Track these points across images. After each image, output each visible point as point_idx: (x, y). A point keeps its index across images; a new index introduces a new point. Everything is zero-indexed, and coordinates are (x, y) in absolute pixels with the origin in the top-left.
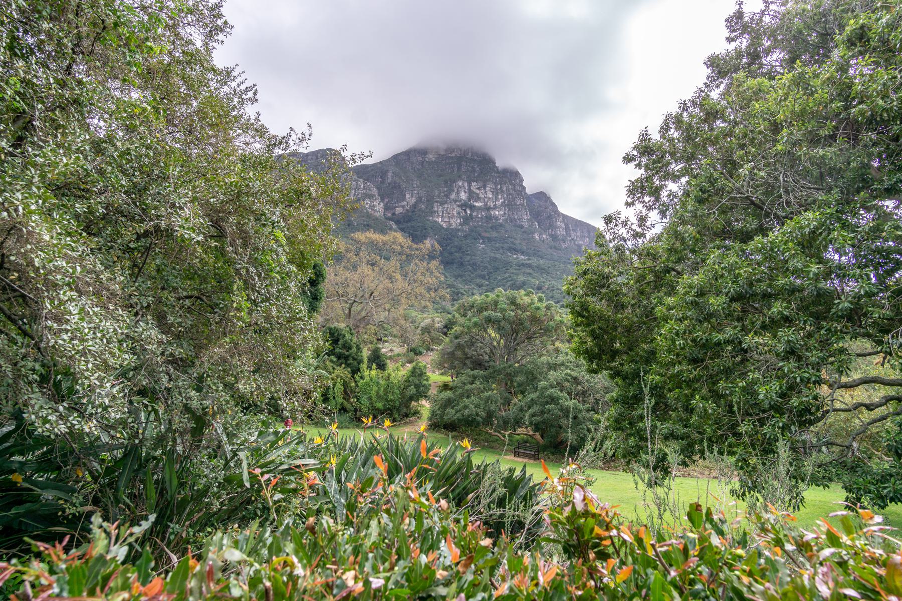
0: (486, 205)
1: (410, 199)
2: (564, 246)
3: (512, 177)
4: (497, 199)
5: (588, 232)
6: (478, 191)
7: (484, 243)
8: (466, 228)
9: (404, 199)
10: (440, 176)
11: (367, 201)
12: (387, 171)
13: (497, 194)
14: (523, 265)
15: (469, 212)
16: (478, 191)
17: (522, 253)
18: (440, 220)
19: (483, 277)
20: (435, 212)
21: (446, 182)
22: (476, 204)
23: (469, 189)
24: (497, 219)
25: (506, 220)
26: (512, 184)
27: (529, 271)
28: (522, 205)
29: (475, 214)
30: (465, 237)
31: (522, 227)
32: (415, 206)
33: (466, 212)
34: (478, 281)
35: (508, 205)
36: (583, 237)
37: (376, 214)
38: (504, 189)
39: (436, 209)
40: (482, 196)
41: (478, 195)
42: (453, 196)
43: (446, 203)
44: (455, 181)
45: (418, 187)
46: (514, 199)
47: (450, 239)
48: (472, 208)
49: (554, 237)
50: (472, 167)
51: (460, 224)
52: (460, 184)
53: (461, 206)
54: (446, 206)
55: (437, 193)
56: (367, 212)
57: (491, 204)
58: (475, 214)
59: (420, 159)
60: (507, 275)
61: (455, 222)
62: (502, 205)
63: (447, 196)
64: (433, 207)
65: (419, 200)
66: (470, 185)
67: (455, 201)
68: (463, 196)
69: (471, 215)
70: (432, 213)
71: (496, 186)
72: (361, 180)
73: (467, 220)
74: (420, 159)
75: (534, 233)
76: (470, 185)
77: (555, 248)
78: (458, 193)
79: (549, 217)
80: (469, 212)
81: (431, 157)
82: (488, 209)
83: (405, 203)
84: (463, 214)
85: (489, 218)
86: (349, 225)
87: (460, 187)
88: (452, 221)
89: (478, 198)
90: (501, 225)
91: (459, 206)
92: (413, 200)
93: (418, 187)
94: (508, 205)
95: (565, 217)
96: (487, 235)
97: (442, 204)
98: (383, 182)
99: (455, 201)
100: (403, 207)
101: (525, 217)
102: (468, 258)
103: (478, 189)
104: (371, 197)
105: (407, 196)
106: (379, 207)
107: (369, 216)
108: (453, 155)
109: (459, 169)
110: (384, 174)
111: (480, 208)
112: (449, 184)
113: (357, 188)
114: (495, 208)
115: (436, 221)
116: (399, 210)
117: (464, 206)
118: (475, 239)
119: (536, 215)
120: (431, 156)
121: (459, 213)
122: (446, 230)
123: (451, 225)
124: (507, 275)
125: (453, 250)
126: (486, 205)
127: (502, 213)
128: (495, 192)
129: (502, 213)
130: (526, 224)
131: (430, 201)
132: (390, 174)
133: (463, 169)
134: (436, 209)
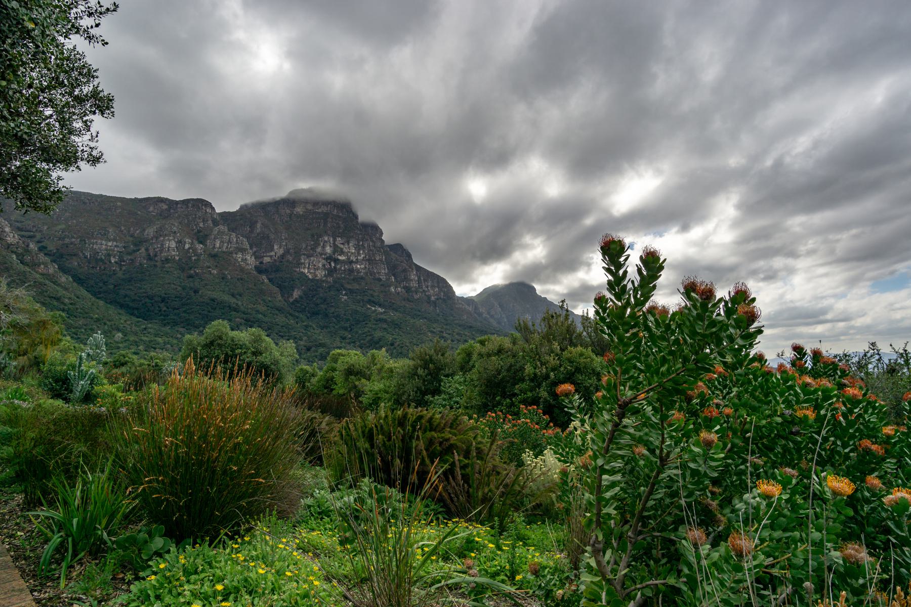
0: (349, 259)
1: (278, 250)
2: (416, 297)
3: (373, 230)
4: (359, 254)
5: (438, 282)
6: (342, 246)
7: (346, 294)
8: (330, 279)
9: (272, 250)
10: (308, 229)
11: (240, 255)
12: (256, 222)
13: (359, 250)
14: (380, 320)
15: (333, 265)
16: (342, 246)
17: (380, 306)
19: (345, 329)
21: (313, 236)
22: (340, 258)
23: (334, 243)
24: (358, 271)
25: (366, 274)
26: (373, 241)
27: (385, 326)
28: (381, 260)
29: (338, 267)
30: (329, 287)
31: (380, 280)
32: (283, 256)
34: (342, 332)
35: (368, 260)
36: (433, 287)
37: (247, 267)
40: (345, 250)
41: (342, 249)
42: (319, 249)
43: (312, 256)
44: (321, 236)
45: (286, 239)
46: (373, 255)
47: (316, 290)
48: (336, 261)
49: (408, 289)
50: (338, 224)
51: (325, 276)
52: (326, 239)
53: (326, 259)
55: (304, 246)
56: (240, 265)
57: (353, 258)
58: (338, 267)
59: (288, 211)
60: (366, 330)
61: (321, 274)
62: (363, 260)
63: (313, 249)
64: (300, 259)
65: (287, 252)
66: (335, 240)
67: (321, 254)
68: (328, 250)
69: (335, 267)
70: (299, 264)
72: (234, 234)
73: (331, 272)
74: (288, 211)
75: (390, 286)
76: (335, 240)
77: (408, 300)
78: (324, 247)
79: (405, 271)
80: (333, 265)
81: (299, 210)
82: (351, 262)
83: (273, 253)
84: (328, 266)
85: (351, 271)
86: (223, 278)
87: (325, 242)
88: (317, 273)
89: (342, 252)
90: (362, 278)
92: (281, 251)
93: (286, 239)
94: (368, 260)
95: (419, 268)
96: (349, 287)
97: (309, 256)
98: (251, 232)
99: (321, 254)
100: (271, 257)
102: (333, 310)
104: (243, 250)
105: (276, 247)
106: (251, 260)
107: (242, 270)
108: (320, 210)
109: (325, 224)
110: (253, 225)
111: (343, 262)
112: (316, 238)
113: (230, 242)
114: (357, 262)
116: (267, 260)
117: (329, 259)
118: (338, 290)
119: (393, 269)
121: (324, 265)
122: (312, 280)
123: (316, 276)
124: (366, 330)
125: (318, 301)
126: (349, 259)
127: (363, 266)
128: (358, 248)
129: (363, 266)
130: (383, 278)
131: (298, 253)
132: (259, 225)
133: (329, 225)
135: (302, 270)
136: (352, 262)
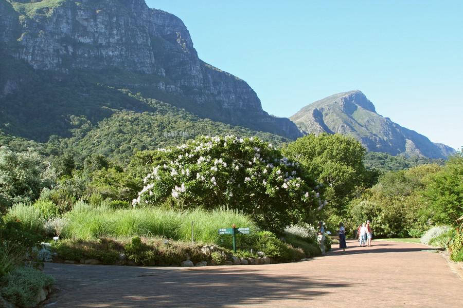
0: (95, 42)
4: (111, 35)
6: (85, 23)
15: (71, 50)
16: (85, 23)
18: (30, 58)
22: (82, 40)
29: (79, 52)
31: (142, 73)
33: (67, 50)
38: (122, 23)
41: (85, 28)
48: (77, 45)
51: (58, 65)
61: (51, 63)
62: (117, 44)
71: (111, 17)
80: (71, 50)
82: (100, 46)
85: (101, 58)
89: (85, 33)
91: (58, 41)
101: (148, 61)
103: (86, 19)
114: (109, 45)
115: (23, 60)
117: (66, 40)
123: (45, 66)
126: (95, 42)
127: (117, 53)
129: (117, 53)
130: (147, 70)
135: (24, 57)
136: (101, 46)
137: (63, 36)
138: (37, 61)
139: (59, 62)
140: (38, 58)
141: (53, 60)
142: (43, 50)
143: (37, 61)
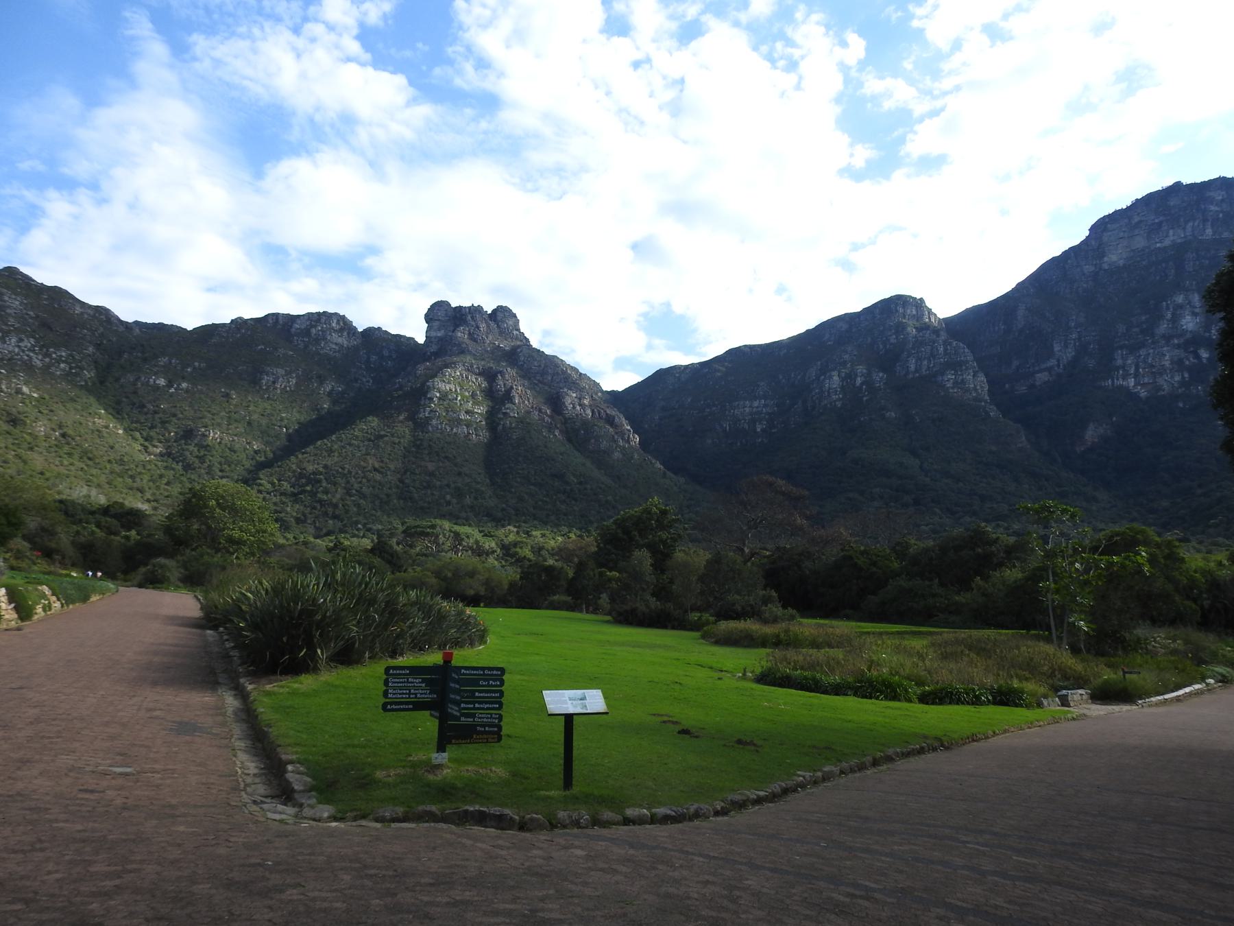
18: (1132, 382)
20: (1118, 369)
33: (1198, 357)
39: (1119, 362)
42: (1163, 328)
51: (1183, 383)
52: (1180, 299)
54: (1143, 352)
61: (1169, 382)
67: (1168, 338)
74: (1088, 269)
78: (1175, 319)
81: (1115, 257)
83: (1053, 362)
87: (1181, 307)
88: (1160, 381)
91: (1179, 346)
92: (1070, 354)
100: (1049, 370)
105: (1057, 348)
108: (1167, 242)
116: (1042, 377)
120: (1114, 258)
123: (1160, 388)
134: (1119, 362)
137: (1188, 336)
138: (1143, 385)
139: (1183, 377)
140: (1146, 380)
141: (1172, 377)
142: (1152, 366)
143: (1143, 385)
